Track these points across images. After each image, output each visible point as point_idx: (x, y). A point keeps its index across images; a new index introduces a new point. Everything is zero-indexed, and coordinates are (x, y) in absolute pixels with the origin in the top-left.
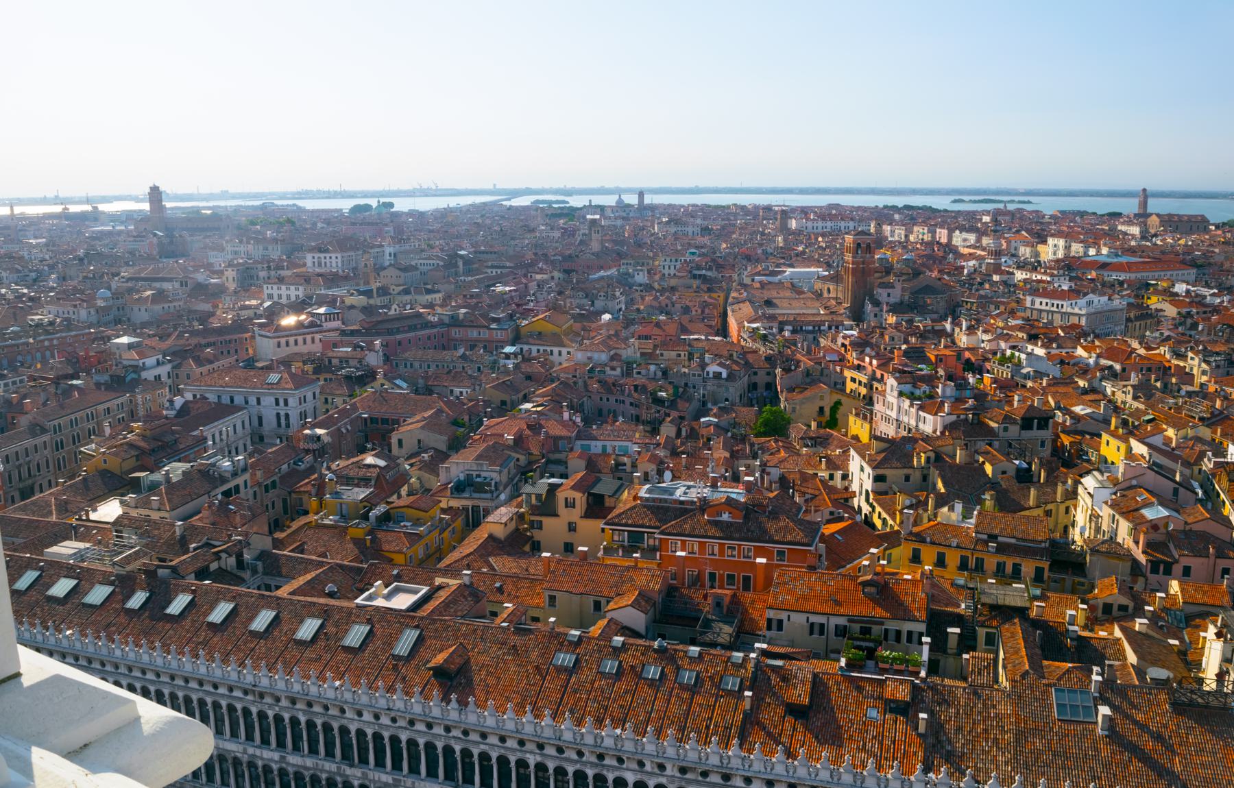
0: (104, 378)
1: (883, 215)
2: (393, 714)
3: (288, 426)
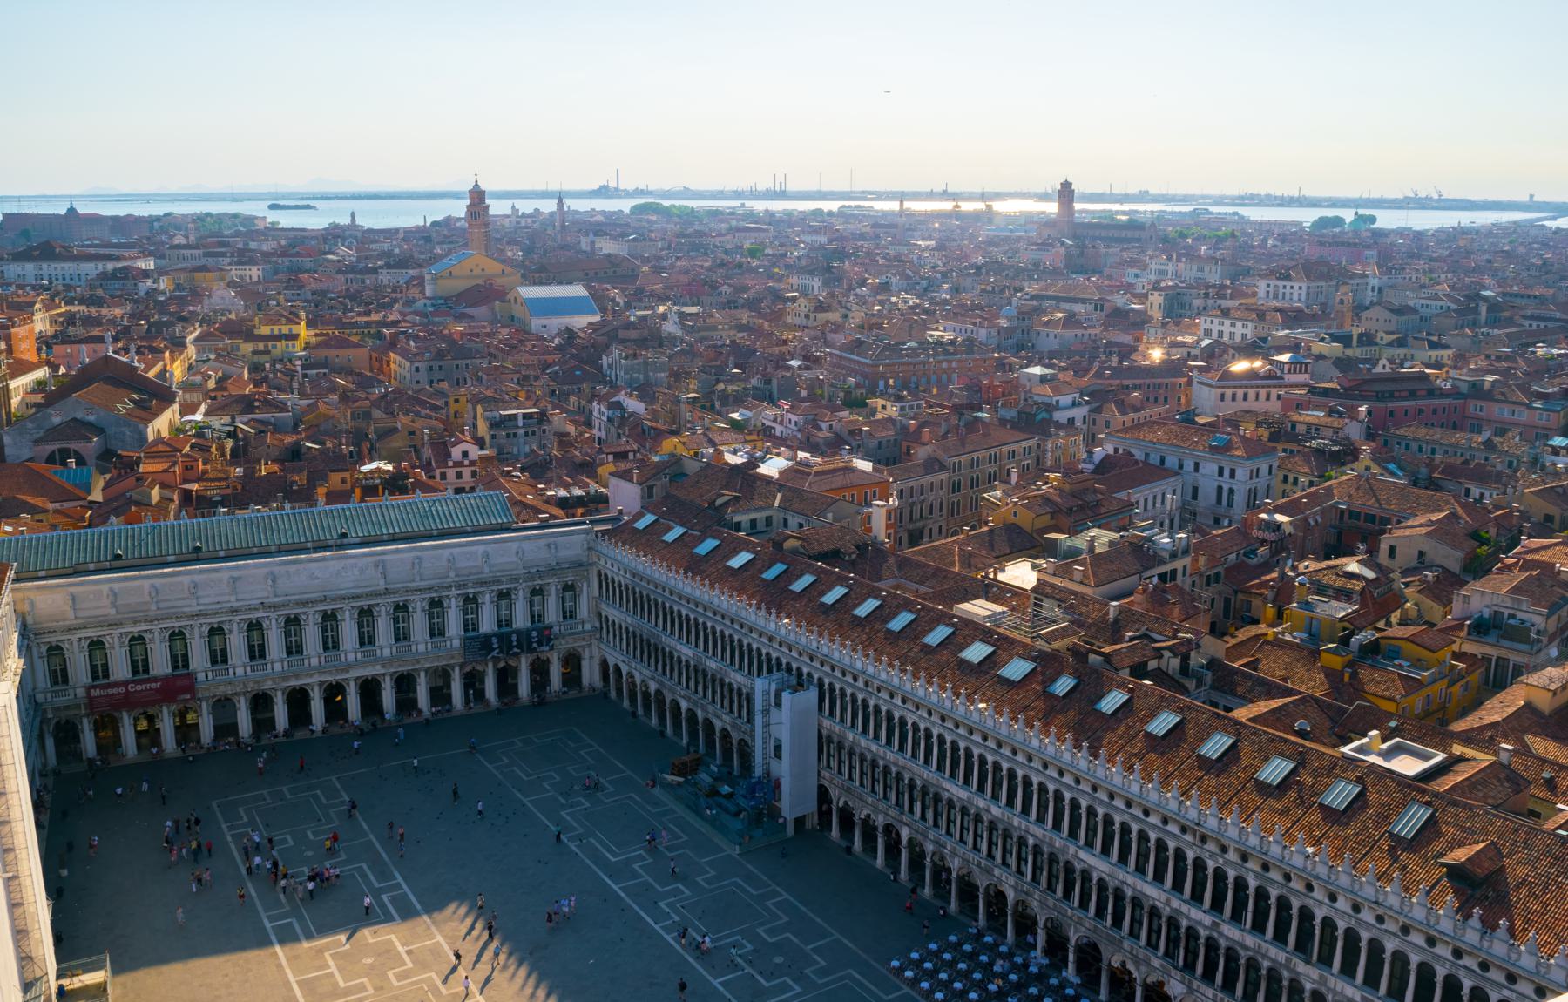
0: (1011, 414)
2: (1381, 911)
3: (1230, 504)
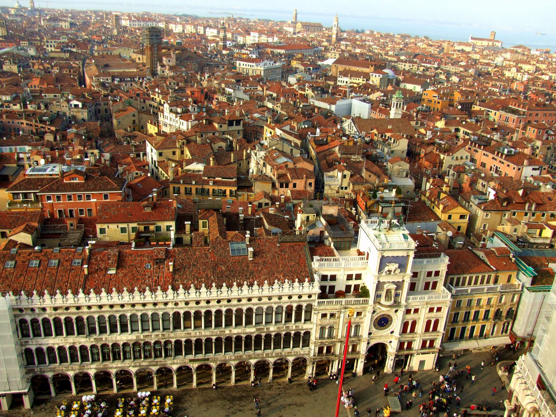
1: (170, 19)
